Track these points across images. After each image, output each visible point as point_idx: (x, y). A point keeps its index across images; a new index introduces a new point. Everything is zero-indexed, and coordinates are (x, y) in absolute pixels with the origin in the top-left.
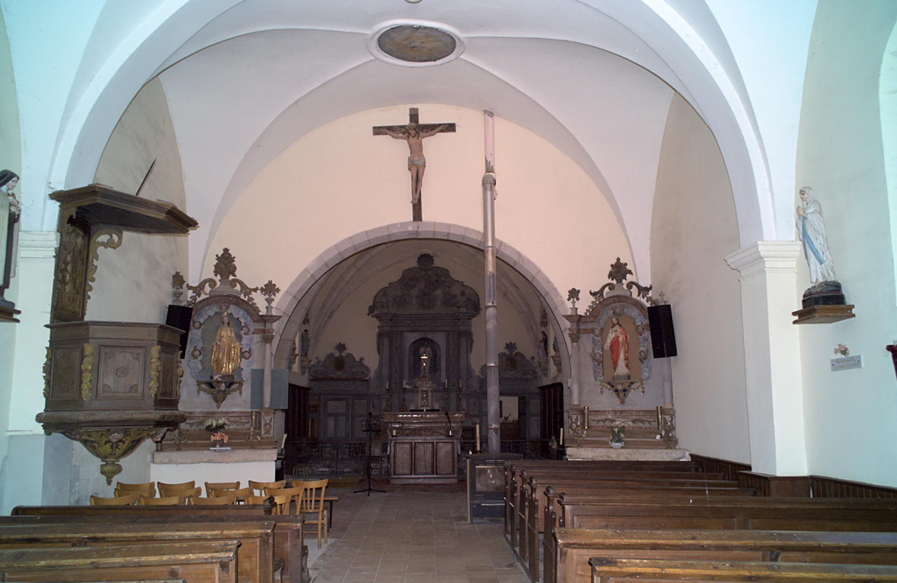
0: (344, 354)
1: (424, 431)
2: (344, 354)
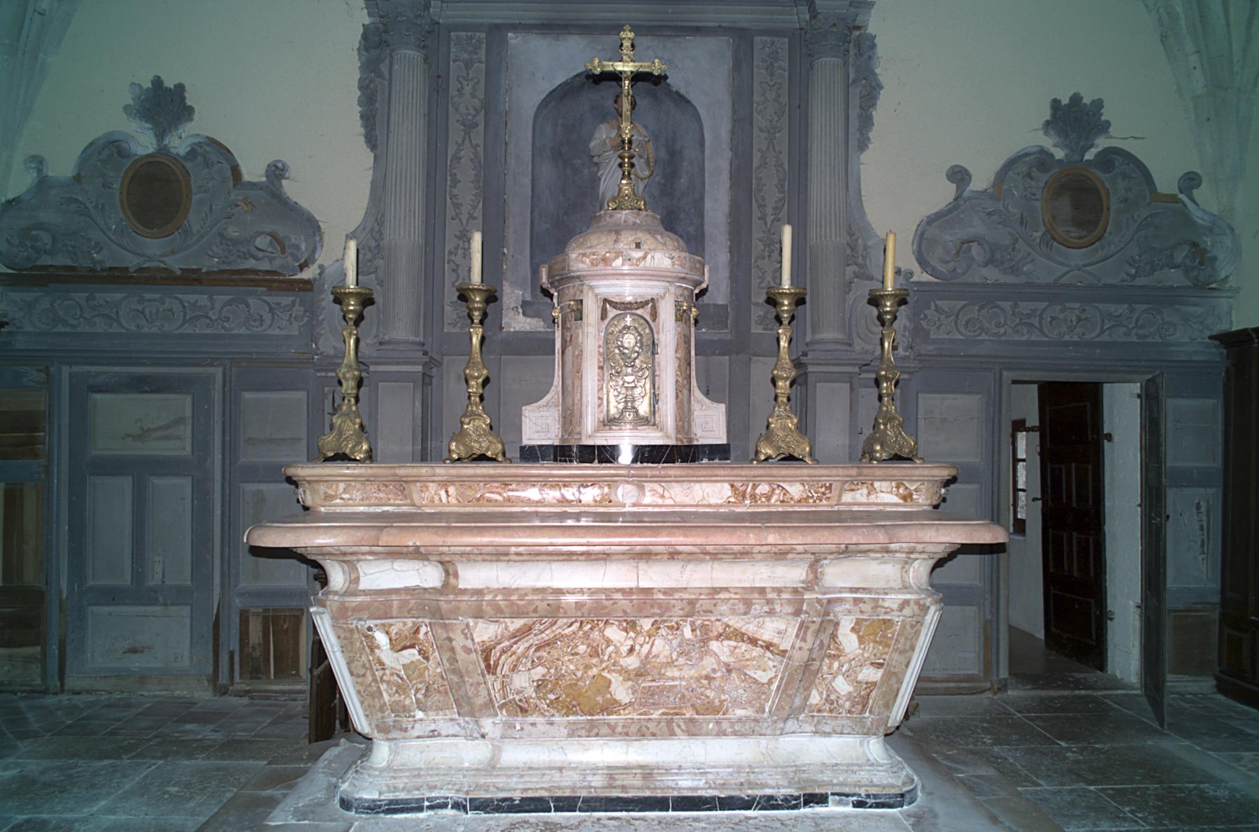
0: (179, 143)
1: (631, 626)
2: (179, 143)
